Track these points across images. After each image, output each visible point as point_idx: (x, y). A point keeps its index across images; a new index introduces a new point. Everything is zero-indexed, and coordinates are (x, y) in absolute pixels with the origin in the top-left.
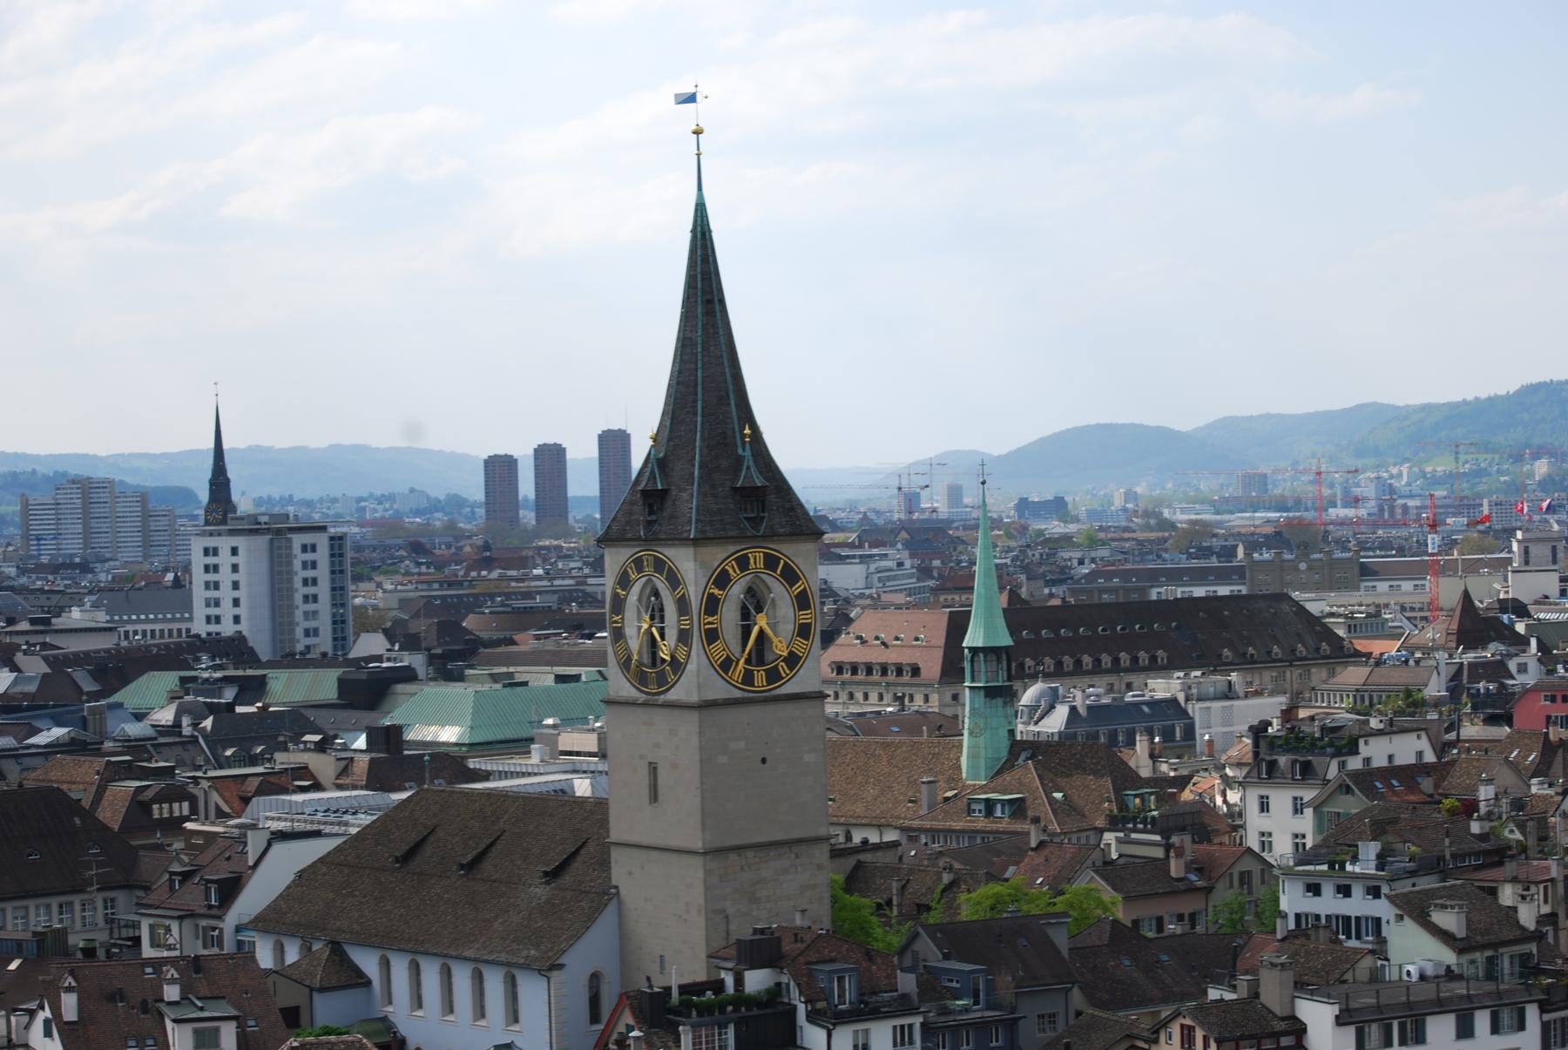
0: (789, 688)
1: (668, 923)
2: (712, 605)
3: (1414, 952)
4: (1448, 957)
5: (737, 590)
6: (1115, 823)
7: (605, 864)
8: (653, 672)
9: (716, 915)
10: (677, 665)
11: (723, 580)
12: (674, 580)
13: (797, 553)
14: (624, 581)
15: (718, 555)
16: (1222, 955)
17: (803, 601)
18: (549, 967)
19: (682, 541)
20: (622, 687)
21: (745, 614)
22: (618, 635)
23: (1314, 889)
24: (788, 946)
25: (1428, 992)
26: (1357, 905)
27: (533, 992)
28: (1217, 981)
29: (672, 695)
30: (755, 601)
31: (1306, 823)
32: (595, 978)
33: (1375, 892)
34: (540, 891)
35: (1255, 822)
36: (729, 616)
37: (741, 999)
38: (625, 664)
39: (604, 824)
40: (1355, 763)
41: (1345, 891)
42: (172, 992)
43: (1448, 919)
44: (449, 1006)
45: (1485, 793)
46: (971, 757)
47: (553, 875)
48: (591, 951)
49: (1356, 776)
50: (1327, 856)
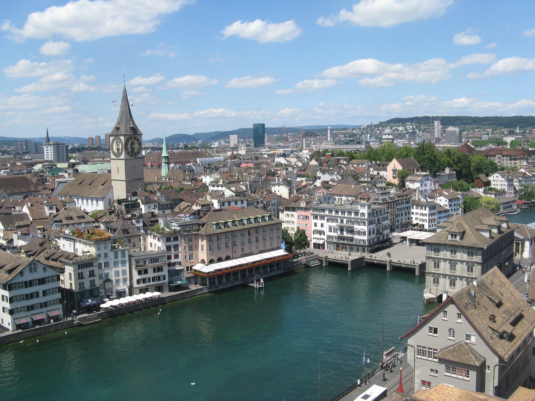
0: (138, 156)
2: (126, 144)
4: (234, 194)
5: (130, 142)
10: (122, 153)
12: (121, 140)
14: (113, 141)
18: (102, 199)
19: (122, 135)
20: (113, 156)
23: (214, 186)
26: (220, 188)
28: (200, 197)
30: (132, 144)
34: (101, 187)
36: (129, 145)
39: (111, 177)
41: (218, 186)
42: (45, 202)
43: (233, 189)
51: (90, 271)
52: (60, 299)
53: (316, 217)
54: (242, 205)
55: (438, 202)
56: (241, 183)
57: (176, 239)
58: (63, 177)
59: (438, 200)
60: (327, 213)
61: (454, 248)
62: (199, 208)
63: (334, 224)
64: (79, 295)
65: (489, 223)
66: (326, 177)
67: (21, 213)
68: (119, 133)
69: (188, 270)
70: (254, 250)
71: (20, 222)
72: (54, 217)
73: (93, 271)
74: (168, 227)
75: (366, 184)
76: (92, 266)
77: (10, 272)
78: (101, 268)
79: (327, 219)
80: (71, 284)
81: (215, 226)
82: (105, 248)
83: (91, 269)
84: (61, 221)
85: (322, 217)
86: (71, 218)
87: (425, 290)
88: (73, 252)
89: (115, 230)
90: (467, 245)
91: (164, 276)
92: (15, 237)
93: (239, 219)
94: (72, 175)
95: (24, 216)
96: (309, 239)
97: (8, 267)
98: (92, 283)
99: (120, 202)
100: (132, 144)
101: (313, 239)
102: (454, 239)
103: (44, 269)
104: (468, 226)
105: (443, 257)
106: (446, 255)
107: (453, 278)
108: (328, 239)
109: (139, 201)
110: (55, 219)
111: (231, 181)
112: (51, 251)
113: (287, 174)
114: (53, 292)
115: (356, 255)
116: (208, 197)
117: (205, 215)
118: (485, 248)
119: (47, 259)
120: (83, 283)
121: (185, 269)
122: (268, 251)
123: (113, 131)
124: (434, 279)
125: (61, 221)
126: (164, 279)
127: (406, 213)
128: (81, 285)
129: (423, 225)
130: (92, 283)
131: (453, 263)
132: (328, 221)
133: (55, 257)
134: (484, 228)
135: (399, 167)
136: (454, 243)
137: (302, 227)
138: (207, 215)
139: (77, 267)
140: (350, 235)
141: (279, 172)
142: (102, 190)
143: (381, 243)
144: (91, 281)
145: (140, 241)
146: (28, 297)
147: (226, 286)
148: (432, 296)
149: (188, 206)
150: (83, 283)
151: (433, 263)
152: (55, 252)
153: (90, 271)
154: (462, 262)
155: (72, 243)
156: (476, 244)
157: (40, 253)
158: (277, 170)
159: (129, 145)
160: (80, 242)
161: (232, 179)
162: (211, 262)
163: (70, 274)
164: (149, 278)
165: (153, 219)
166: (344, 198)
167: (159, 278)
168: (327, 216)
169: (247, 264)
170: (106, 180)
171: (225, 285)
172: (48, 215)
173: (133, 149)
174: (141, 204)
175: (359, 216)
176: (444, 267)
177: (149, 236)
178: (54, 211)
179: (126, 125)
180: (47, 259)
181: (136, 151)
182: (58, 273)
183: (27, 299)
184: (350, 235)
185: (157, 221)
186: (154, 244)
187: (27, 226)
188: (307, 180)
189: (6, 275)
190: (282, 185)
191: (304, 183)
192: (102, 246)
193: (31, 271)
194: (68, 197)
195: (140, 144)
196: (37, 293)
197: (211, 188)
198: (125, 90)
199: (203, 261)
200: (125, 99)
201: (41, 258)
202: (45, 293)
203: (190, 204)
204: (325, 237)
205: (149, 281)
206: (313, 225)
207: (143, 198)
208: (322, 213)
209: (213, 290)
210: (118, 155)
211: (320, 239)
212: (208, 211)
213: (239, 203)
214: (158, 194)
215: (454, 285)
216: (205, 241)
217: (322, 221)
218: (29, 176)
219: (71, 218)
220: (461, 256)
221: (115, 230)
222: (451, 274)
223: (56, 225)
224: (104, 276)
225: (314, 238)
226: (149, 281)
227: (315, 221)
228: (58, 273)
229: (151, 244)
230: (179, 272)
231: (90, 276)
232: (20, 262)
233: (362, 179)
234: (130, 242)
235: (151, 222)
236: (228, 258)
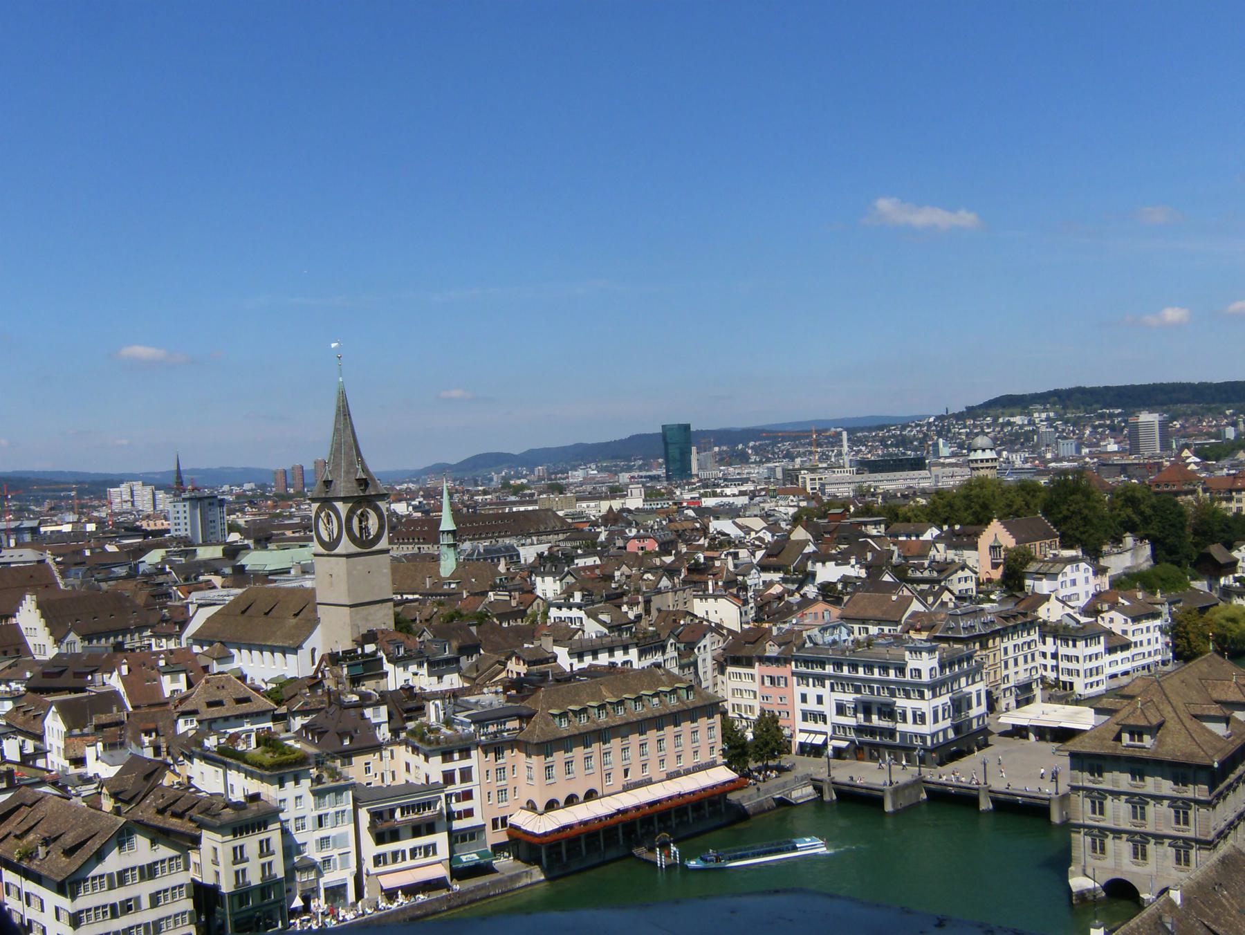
2: (349, 519)
3: (592, 629)
4: (606, 631)
7: (315, 611)
8: (330, 545)
9: (354, 626)
21: (360, 522)
24: (379, 636)
29: (337, 551)
30: (363, 517)
32: (313, 650)
34: (293, 621)
36: (355, 521)
37: (364, 655)
39: (314, 597)
41: (570, 608)
43: (605, 617)
45: (617, 574)
47: (296, 615)
52: (191, 913)
53: (803, 677)
54: (626, 658)
55: (1107, 625)
57: (465, 753)
58: (210, 586)
59: (1107, 619)
60: (829, 669)
61: (1139, 766)
62: (523, 669)
63: (849, 697)
64: (236, 900)
65: (1223, 698)
66: (828, 573)
67: (104, 690)
68: (330, 495)
69: (495, 826)
70: (653, 771)
71: (103, 716)
75: (926, 587)
79: (832, 685)
80: (217, 873)
83: (263, 836)
84: (194, 712)
85: (820, 679)
86: (219, 703)
87: (1072, 868)
88: (222, 791)
90: (1169, 758)
92: (90, 753)
93: (614, 700)
94: (229, 582)
95: (112, 698)
96: (786, 732)
97: (69, 840)
101: (801, 733)
102: (1137, 743)
104: (1170, 709)
105: (1110, 788)
106: (1115, 782)
107: (1137, 838)
108: (834, 732)
109: (381, 654)
110: (180, 709)
113: (736, 566)
115: (904, 774)
118: (1216, 765)
119: (161, 811)
120: (244, 871)
121: (489, 827)
122: (688, 772)
124: (1094, 842)
125: (194, 712)
127: (1026, 658)
129: (1071, 684)
131: (1138, 802)
132: (832, 690)
133: (179, 808)
134: (1212, 713)
135: (1008, 541)
136: (1138, 753)
137: (773, 706)
140: (885, 724)
141: (717, 563)
142: (296, 627)
143: (966, 740)
144: (263, 866)
146: (115, 911)
148: (1088, 884)
150: (244, 871)
151: (1088, 802)
152: (181, 793)
154: (1158, 799)
156: (1192, 755)
158: (713, 559)
159: (355, 521)
160: (239, 769)
162: (551, 805)
165: (412, 704)
166: (874, 630)
168: (830, 677)
169: (637, 808)
172: (167, 694)
174: (385, 660)
175: (908, 678)
176: (1118, 813)
178: (182, 684)
179: (347, 472)
180: (161, 811)
184: (885, 724)
187: (119, 724)
188: (784, 580)
190: (722, 596)
191: (777, 589)
194: (217, 645)
196: (138, 899)
199: (531, 806)
200: (344, 412)
202: (155, 900)
203: (503, 658)
204: (828, 728)
206: (798, 698)
208: (818, 670)
211: (816, 733)
214: (428, 636)
215: (1144, 856)
217: (819, 690)
218: (128, 588)
219: (219, 703)
220: (1152, 785)
222: (1133, 828)
225: (801, 731)
226: (404, 859)
227: (803, 689)
229: (408, 765)
230: (473, 834)
231: (261, 856)
233: (918, 574)
235: (408, 711)
236: (590, 795)
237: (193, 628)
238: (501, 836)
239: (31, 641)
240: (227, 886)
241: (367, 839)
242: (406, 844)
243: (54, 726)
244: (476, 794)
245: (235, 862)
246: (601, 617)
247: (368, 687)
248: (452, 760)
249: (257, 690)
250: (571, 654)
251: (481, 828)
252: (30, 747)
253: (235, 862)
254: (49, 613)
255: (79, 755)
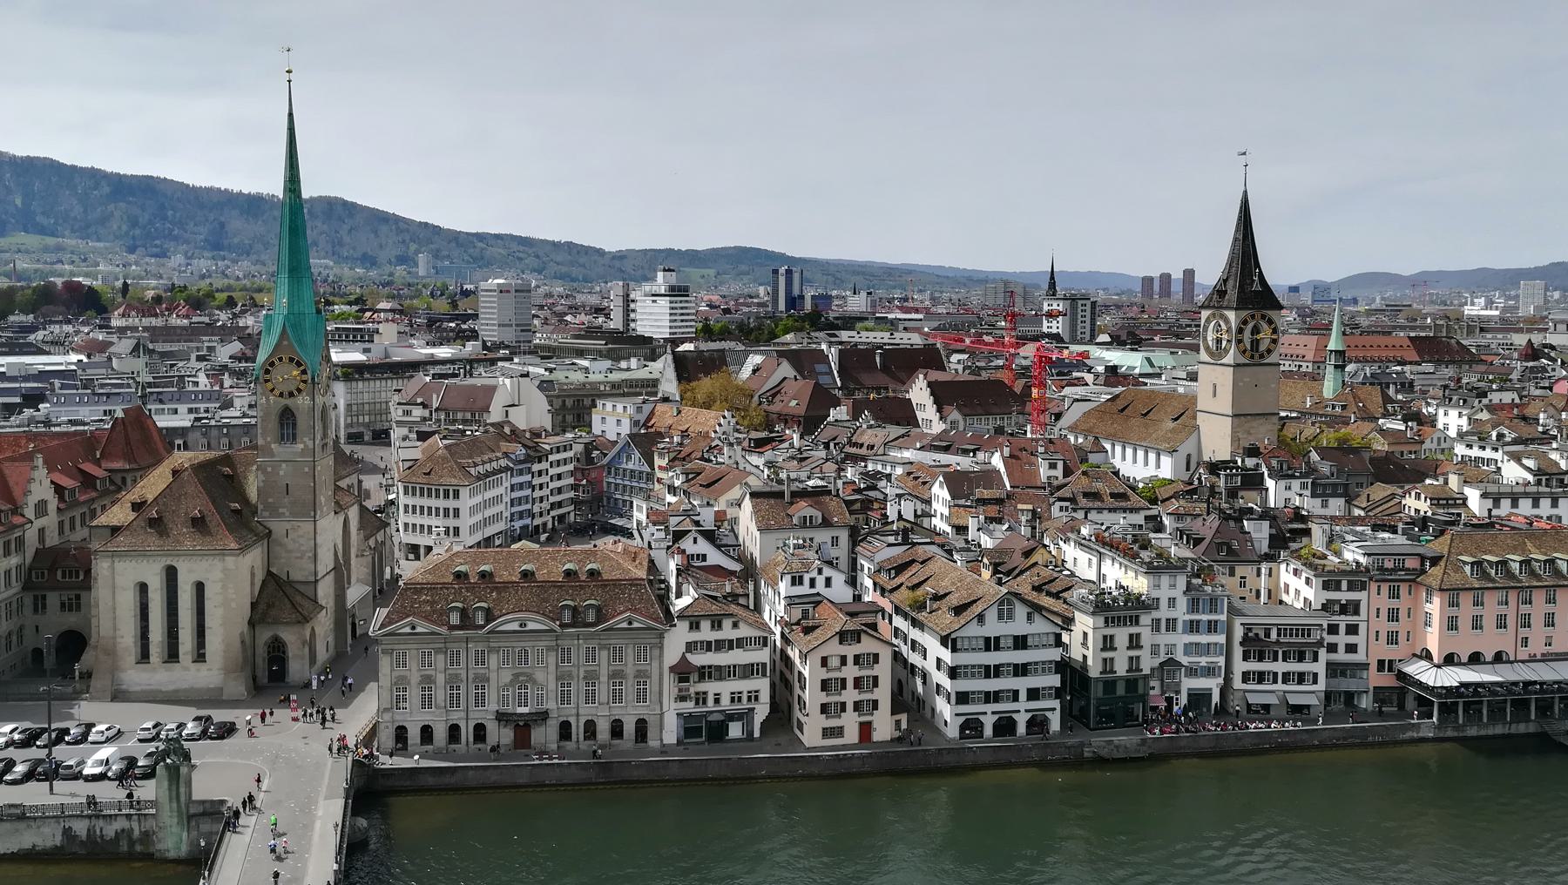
1: (1217, 438)
2: (1240, 331)
3: (1513, 473)
4: (1530, 478)
5: (1250, 325)
6: (1384, 416)
7: (1195, 418)
9: (1235, 439)
10: (1227, 351)
11: (1245, 322)
12: (1227, 321)
13: (1272, 314)
14: (1208, 321)
15: (1244, 313)
16: (1431, 468)
17: (1275, 331)
18: (1172, 452)
20: (1204, 356)
22: (1205, 339)
23: (1470, 446)
25: (1521, 489)
26: (1488, 454)
27: (1166, 461)
29: (1224, 361)
30: (1256, 330)
31: (1464, 421)
33: (1496, 450)
34: (1171, 425)
35: (1441, 421)
37: (1244, 469)
38: (1207, 348)
40: (1485, 401)
41: (1483, 448)
42: (1041, 450)
43: (1530, 463)
44: (1135, 461)
46: (1329, 388)
48: (1187, 447)
49: (1487, 406)
50: (1476, 434)
51: (1131, 636)
56: (1555, 445)
58: (1081, 382)
62: (1424, 506)
64: (1101, 686)
72: (1059, 488)
73: (1138, 635)
74: (1338, 554)
76: (1137, 623)
77: (959, 610)
78: (1158, 630)
81: (1468, 569)
82: (1173, 586)
83: (1134, 630)
89: (1197, 542)
91: (1315, 675)
92: (972, 524)
93: (1543, 558)
94: (1102, 379)
95: (990, 476)
97: (954, 600)
98: (1134, 663)
99: (1214, 468)
100: (1256, 330)
103: (1029, 617)
111: (1525, 436)
112: (1047, 573)
114: (1044, 670)
116: (1454, 481)
117: (1442, 533)
120: (1112, 659)
123: (1210, 298)
125: (1072, 500)
126: (1315, 682)
128: (1108, 665)
130: (1134, 663)
138: (1447, 537)
139: (1101, 621)
142: (1173, 431)
144: (1131, 658)
145: (1259, 575)
147: (1490, 732)
149: (1393, 495)
150: (1112, 659)
153: (1131, 636)
155: (1095, 560)
157: (1022, 572)
161: (1527, 431)
162: (1450, 660)
163: (1085, 634)
164: (1275, 674)
167: (1301, 678)
170: (1185, 413)
171: (1486, 726)
172: (1044, 479)
173: (1255, 344)
177: (1283, 566)
178: (1059, 472)
181: (1263, 348)
182: (1058, 630)
183: (987, 676)
185: (1307, 532)
186: (1297, 588)
187: (999, 501)
189: (950, 617)
192: (1165, 580)
193: (1000, 617)
195: (1275, 331)
197: (1460, 450)
198: (1245, 192)
201: (1023, 585)
205: (1275, 681)
207: (1274, 463)
209: (1450, 733)
210: (1217, 353)
212: (1452, 523)
213: (1545, 503)
216: (1436, 600)
221: (1197, 542)
223: (1061, 509)
224: (1162, 650)
228: (1058, 630)
232: (980, 593)
234: (1232, 574)
235: (1291, 531)
237: (1065, 421)
238: (1387, 680)
239: (920, 415)
240: (1094, 671)
241: (1238, 652)
242: (1280, 667)
243: (940, 493)
244: (1362, 628)
245: (1104, 649)
246: (1525, 461)
247: (1250, 500)
248: (1338, 588)
249: (1134, 489)
250: (1484, 496)
251: (1365, 666)
252: (920, 507)
253: (1104, 649)
254: (942, 395)
255: (961, 522)
